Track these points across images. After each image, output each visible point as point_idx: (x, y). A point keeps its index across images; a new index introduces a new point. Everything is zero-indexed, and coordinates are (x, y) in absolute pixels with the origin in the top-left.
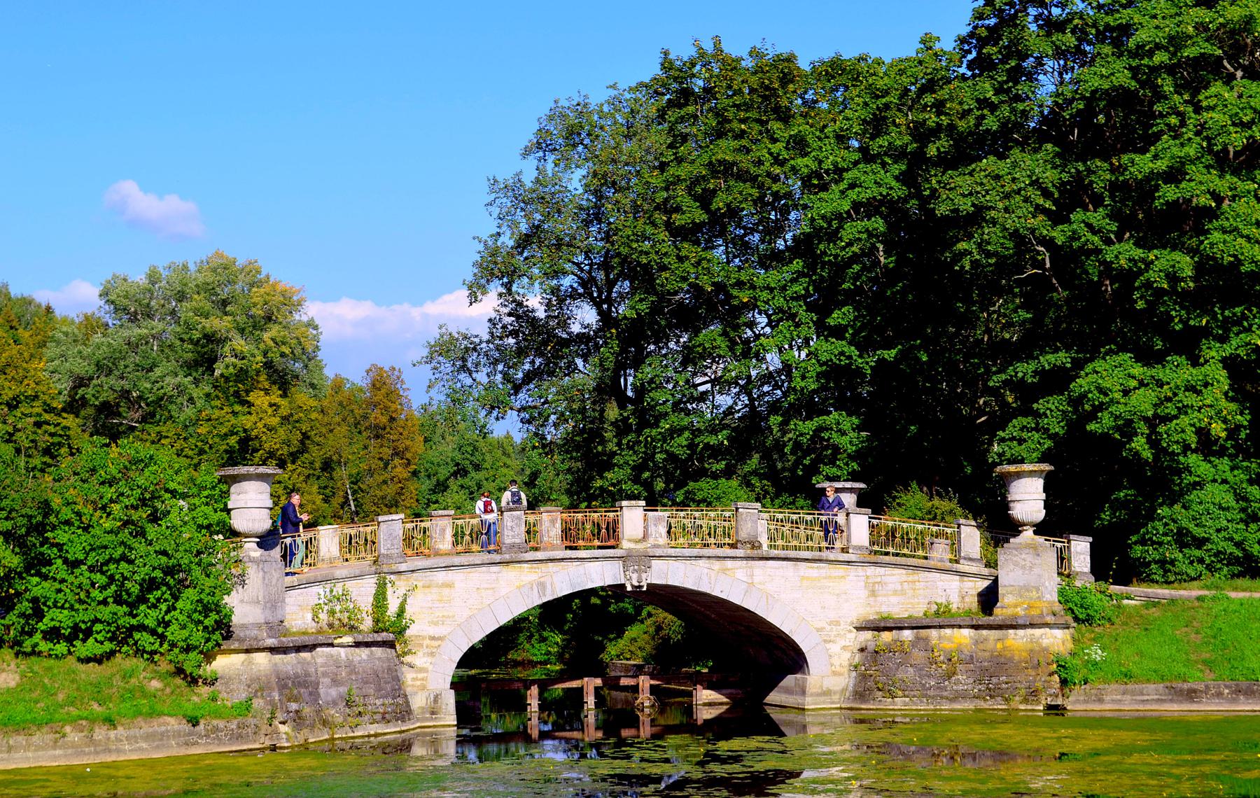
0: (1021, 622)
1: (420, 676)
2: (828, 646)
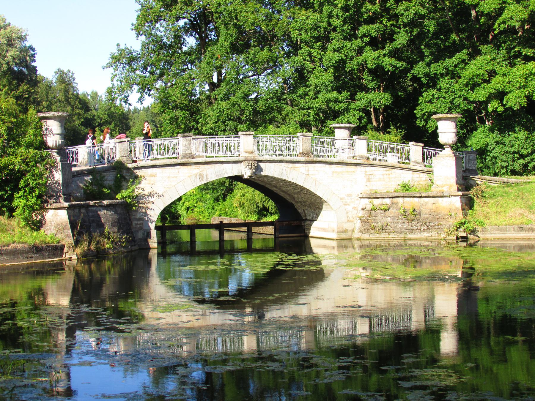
0: (445, 194)
1: (139, 222)
2: (346, 207)
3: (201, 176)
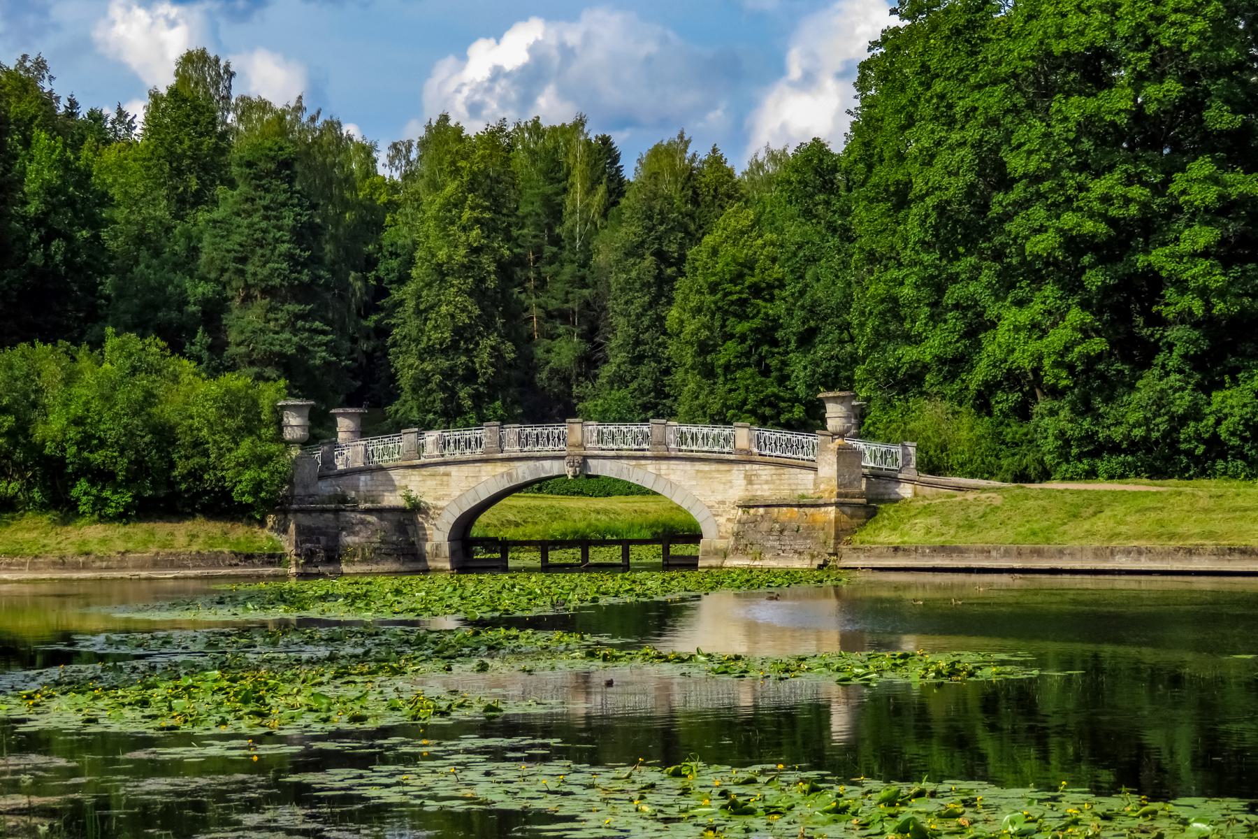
0: (821, 502)
3: (510, 475)
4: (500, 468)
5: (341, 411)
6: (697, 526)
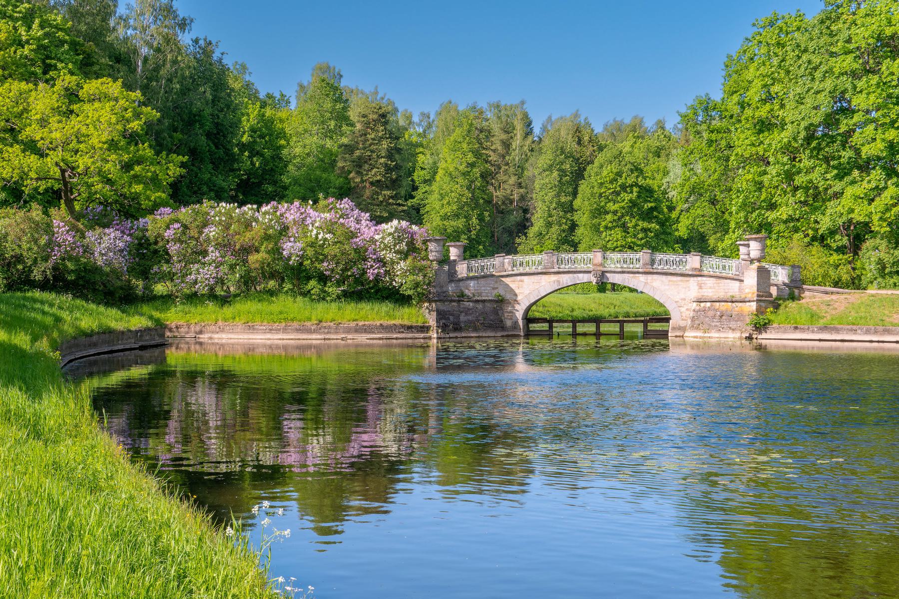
0: (747, 300)
3: (559, 282)
4: (554, 278)
5: (453, 244)
6: (667, 312)
